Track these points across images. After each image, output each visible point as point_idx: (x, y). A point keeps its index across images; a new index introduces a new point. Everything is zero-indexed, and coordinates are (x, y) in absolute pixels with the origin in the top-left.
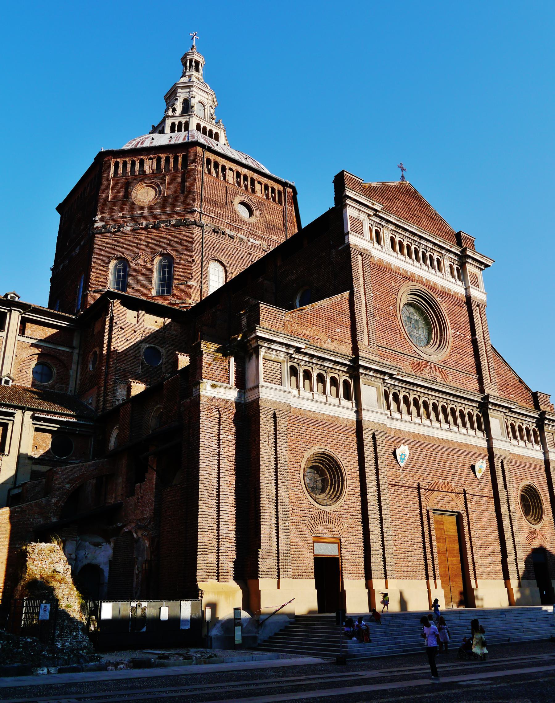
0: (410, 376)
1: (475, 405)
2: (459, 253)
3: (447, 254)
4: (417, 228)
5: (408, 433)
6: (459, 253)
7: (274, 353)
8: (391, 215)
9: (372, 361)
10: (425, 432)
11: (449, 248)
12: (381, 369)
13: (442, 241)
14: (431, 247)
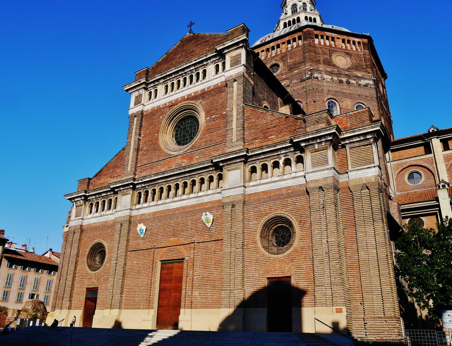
0: (145, 177)
1: (212, 169)
2: (216, 53)
3: (209, 61)
4: (174, 68)
5: (149, 214)
6: (216, 53)
7: (78, 202)
8: (156, 76)
9: (115, 183)
10: (162, 208)
11: (205, 58)
12: (122, 184)
13: (196, 59)
14: (194, 68)
